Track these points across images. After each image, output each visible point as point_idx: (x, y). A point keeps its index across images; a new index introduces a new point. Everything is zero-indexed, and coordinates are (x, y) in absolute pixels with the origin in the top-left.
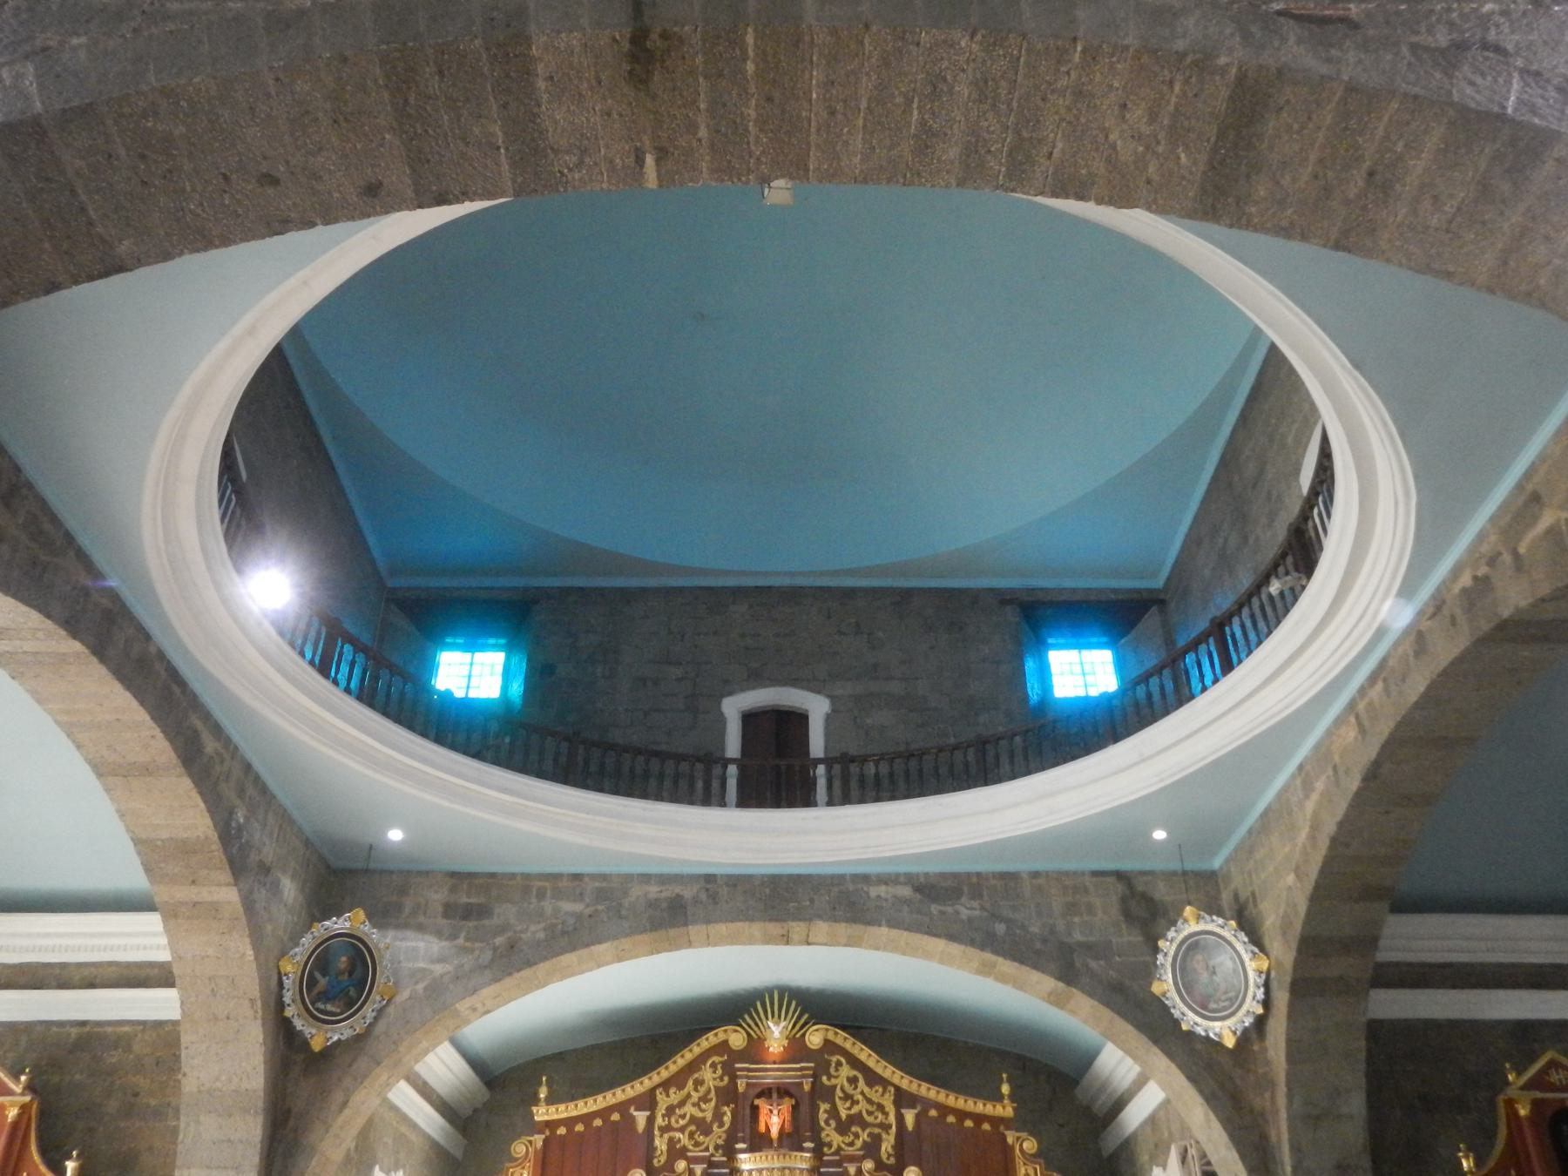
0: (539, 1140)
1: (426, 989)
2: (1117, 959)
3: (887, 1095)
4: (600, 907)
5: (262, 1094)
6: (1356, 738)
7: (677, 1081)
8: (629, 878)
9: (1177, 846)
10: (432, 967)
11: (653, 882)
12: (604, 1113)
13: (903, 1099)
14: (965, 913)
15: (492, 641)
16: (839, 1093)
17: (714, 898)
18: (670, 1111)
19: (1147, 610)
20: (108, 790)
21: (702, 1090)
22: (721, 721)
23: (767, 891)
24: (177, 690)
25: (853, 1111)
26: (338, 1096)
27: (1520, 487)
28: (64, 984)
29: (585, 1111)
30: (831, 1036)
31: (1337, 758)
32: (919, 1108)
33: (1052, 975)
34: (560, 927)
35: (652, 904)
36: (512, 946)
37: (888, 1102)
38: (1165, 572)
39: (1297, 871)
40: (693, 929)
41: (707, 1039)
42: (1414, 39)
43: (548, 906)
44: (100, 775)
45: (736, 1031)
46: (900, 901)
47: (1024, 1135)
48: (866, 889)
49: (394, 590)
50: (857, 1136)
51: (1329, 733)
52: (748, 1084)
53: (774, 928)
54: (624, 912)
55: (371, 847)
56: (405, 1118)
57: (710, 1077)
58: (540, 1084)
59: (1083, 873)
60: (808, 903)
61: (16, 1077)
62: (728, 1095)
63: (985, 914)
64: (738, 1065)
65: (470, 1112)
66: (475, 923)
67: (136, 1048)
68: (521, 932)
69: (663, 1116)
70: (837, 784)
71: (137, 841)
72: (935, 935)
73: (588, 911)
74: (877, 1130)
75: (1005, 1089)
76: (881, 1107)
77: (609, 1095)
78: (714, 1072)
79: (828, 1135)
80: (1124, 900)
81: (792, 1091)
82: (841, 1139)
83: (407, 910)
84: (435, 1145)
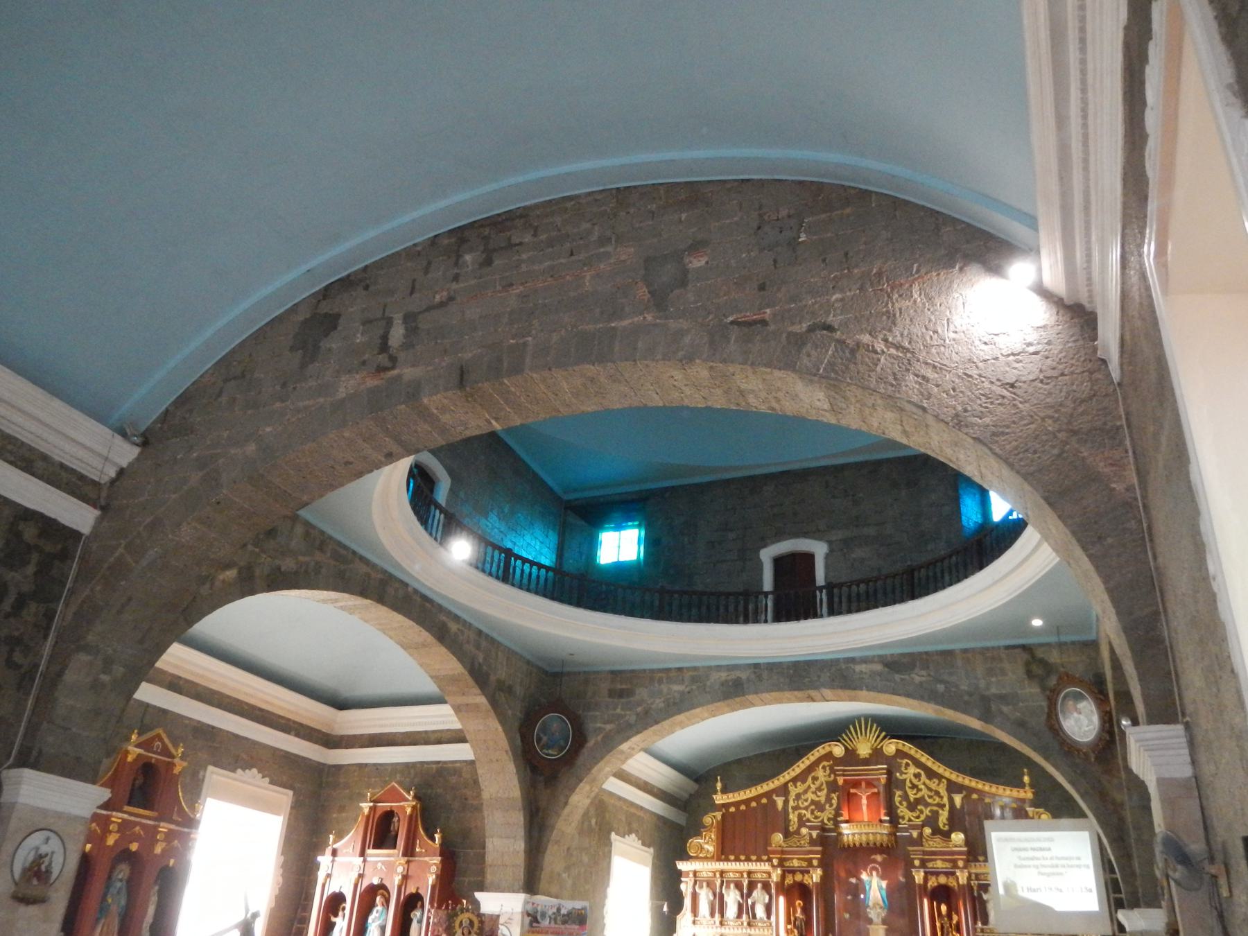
0: (719, 815)
2: (1021, 704)
3: (941, 785)
4: (694, 687)
7: (801, 778)
8: (710, 668)
9: (1054, 627)
10: (602, 726)
12: (757, 798)
13: (953, 787)
14: (917, 679)
15: (630, 524)
16: (908, 784)
17: (759, 677)
18: (798, 797)
21: (818, 783)
22: (759, 566)
23: (791, 671)
24: (428, 605)
26: (562, 799)
28: (427, 743)
29: (745, 797)
30: (900, 747)
32: (964, 793)
35: (722, 684)
36: (647, 712)
37: (942, 790)
41: (818, 751)
42: (790, 329)
44: (405, 649)
45: (836, 745)
46: (873, 674)
47: (1041, 810)
49: (569, 501)
50: (921, 812)
52: (845, 780)
54: (708, 690)
55: (563, 661)
56: (632, 804)
57: (821, 774)
58: (717, 781)
59: (999, 648)
62: (833, 787)
63: (931, 679)
64: (836, 768)
65: (686, 796)
67: (463, 774)
68: (652, 704)
69: (794, 800)
71: (432, 677)
73: (687, 689)
74: (935, 808)
75: (1026, 779)
76: (937, 793)
77: (759, 788)
80: (1027, 664)
81: (875, 783)
82: (910, 814)
84: (660, 818)
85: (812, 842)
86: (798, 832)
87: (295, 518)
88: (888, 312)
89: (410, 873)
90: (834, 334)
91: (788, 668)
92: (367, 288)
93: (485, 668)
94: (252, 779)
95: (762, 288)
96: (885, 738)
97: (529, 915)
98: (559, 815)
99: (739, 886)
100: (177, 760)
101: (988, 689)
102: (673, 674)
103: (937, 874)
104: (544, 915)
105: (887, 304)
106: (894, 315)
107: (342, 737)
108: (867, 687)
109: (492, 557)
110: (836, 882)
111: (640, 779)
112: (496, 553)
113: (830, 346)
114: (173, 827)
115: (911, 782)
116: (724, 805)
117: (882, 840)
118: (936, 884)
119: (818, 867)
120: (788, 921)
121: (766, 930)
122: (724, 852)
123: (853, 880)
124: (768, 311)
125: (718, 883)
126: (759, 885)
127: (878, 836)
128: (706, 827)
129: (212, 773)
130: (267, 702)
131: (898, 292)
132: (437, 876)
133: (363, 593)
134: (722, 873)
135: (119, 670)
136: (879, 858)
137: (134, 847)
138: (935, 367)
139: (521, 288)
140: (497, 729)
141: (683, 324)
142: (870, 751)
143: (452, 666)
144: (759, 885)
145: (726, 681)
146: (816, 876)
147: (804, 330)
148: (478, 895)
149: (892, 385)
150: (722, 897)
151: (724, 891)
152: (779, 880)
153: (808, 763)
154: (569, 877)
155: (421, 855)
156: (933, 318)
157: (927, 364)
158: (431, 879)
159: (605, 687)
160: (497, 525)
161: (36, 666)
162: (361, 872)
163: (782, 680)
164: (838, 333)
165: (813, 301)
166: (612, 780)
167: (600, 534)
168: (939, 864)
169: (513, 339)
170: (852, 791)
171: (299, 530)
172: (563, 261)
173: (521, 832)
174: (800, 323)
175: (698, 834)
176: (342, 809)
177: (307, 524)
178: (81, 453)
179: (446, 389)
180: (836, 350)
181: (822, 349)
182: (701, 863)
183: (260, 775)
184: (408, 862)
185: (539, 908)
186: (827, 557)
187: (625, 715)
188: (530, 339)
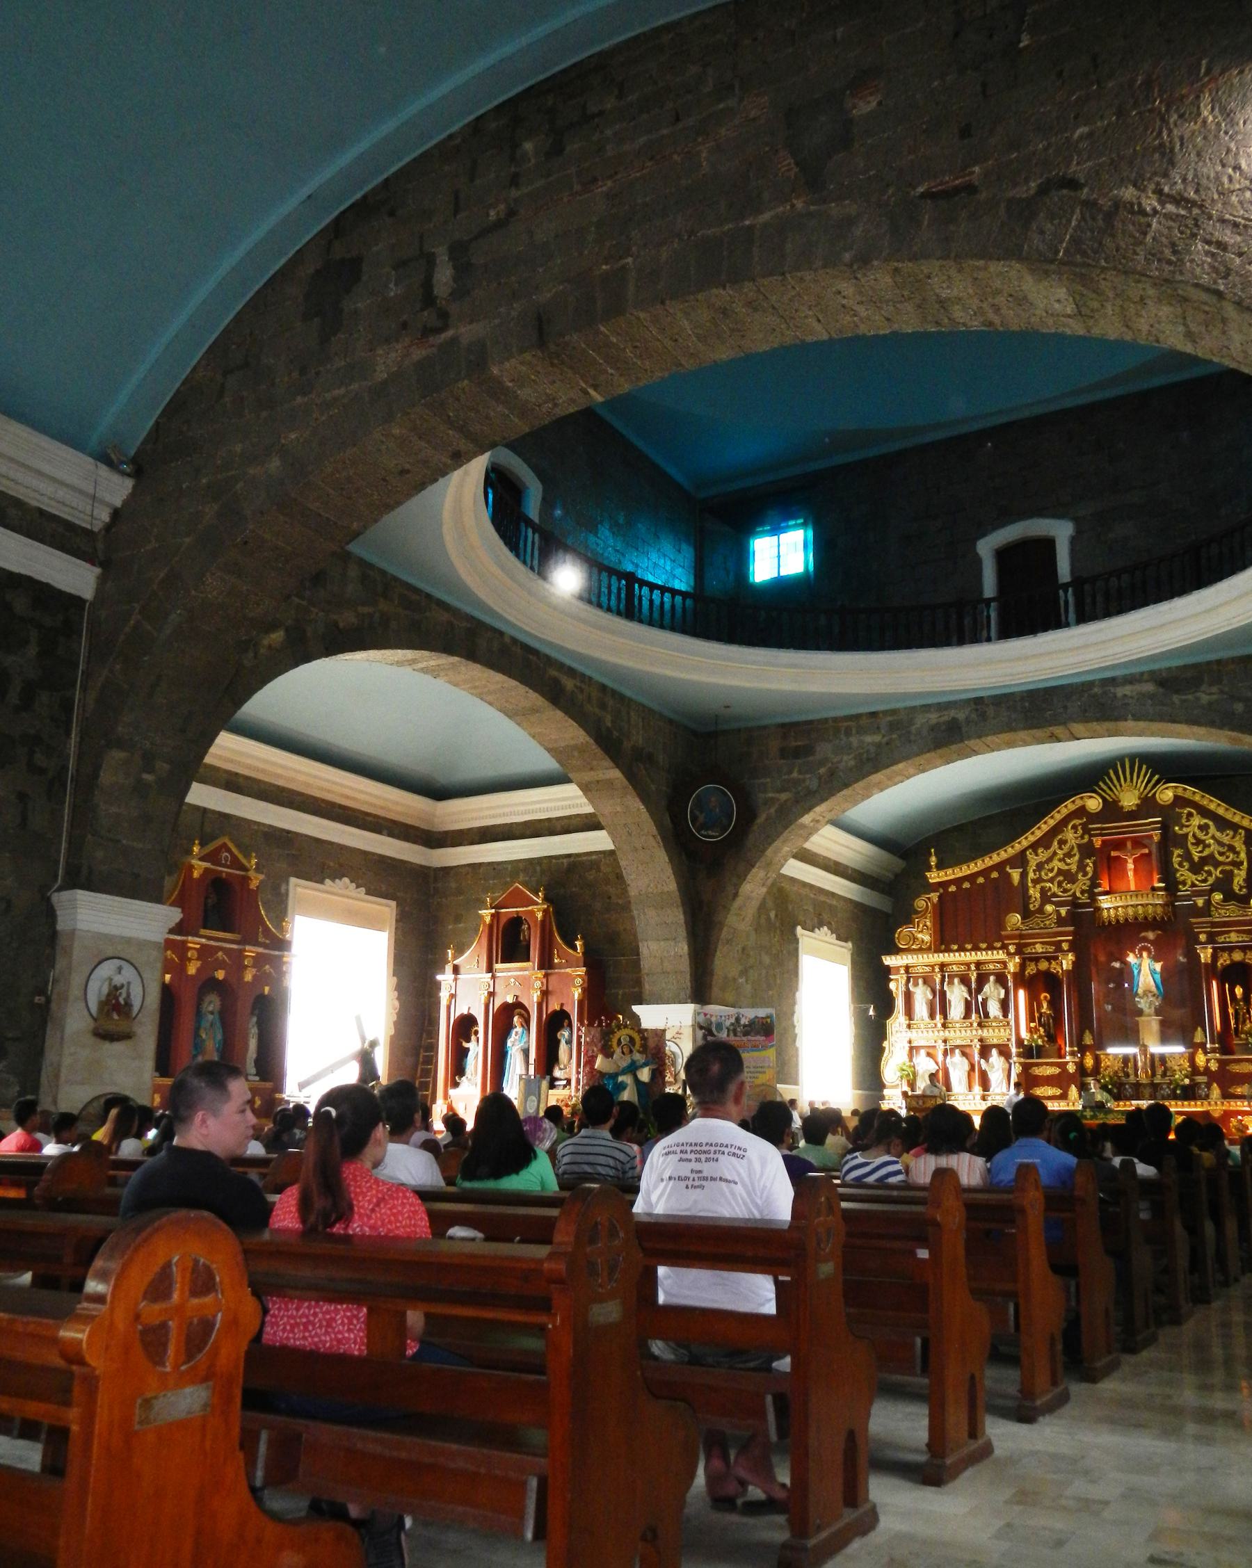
0: (935, 896)
1: (776, 811)
3: (1238, 838)
4: (894, 736)
5: (677, 893)
7: (1044, 842)
8: (914, 708)
12: (985, 872)
14: (1205, 699)
15: (792, 523)
16: (1191, 839)
17: (983, 716)
18: (1040, 867)
20: (519, 724)
21: (1066, 848)
23: (1027, 704)
25: (1206, 853)
29: (969, 872)
30: (1180, 792)
34: (865, 755)
35: (933, 729)
36: (832, 773)
41: (1066, 806)
42: (1010, 194)
44: (510, 717)
45: (1091, 797)
46: (1142, 696)
48: (1112, 690)
50: (1210, 873)
52: (1103, 841)
53: (1038, 733)
54: (913, 738)
58: (930, 854)
60: (1061, 710)
61: (537, 896)
62: (1086, 850)
65: (892, 876)
67: (602, 868)
69: (1034, 871)
71: (549, 750)
73: (885, 739)
76: (1232, 848)
77: (987, 859)
78: (1076, 833)
79: (1182, 875)
81: (1146, 841)
82: (1194, 877)
85: (1061, 921)
86: (1041, 910)
87: (346, 557)
88: (1162, 145)
89: (550, 988)
90: (1079, 192)
91: (1022, 699)
92: (392, 214)
93: (616, 734)
94: (343, 891)
95: (965, 132)
96: (1158, 782)
97: (701, 1028)
98: (727, 909)
99: (965, 981)
100: (252, 874)
102: (863, 722)
103: (1231, 950)
104: (719, 1026)
105: (1160, 133)
106: (1172, 150)
107: (446, 833)
108: (1133, 715)
109: (609, 587)
110: (1094, 970)
111: (829, 859)
112: (614, 579)
113: (1073, 213)
114: (260, 950)
115: (1194, 836)
116: (940, 884)
117: (1155, 912)
118: (1228, 962)
119: (1069, 951)
120: (1031, 1018)
121: (1002, 1030)
122: (942, 942)
123: (1117, 965)
124: (977, 169)
125: (938, 979)
126: (992, 978)
127: (1150, 909)
128: (918, 912)
129: (296, 885)
130: (348, 797)
131: (1177, 110)
132: (584, 990)
133: (448, 649)
134: (943, 966)
135: (163, 767)
136: (1151, 935)
137: (220, 975)
138: (1236, 225)
139: (609, 183)
140: (638, 810)
141: (851, 208)
142: (1137, 802)
143: (573, 734)
144: (992, 978)
146: (1067, 962)
147: (1032, 192)
148: (636, 1009)
149: (1169, 262)
150: (943, 994)
151: (946, 988)
152: (1017, 970)
153: (1052, 823)
154: (747, 981)
155: (560, 966)
156: (1233, 146)
157: (1223, 221)
158: (577, 993)
159: (774, 745)
160: (611, 542)
161: (65, 768)
162: (491, 990)
163: (1013, 716)
164: (1086, 190)
165: (1045, 143)
166: (792, 862)
167: (751, 542)
168: (1233, 937)
169: (606, 264)
170: (1113, 854)
171: (353, 572)
172: (665, 132)
173: (682, 933)
174: (1027, 180)
175: (908, 921)
176: (458, 919)
177: (362, 563)
178: (61, 493)
179: (522, 351)
180: (1083, 218)
181: (1060, 219)
182: (915, 956)
183: (354, 885)
184: (546, 976)
185: (713, 1019)
187: (804, 781)
188: (630, 260)
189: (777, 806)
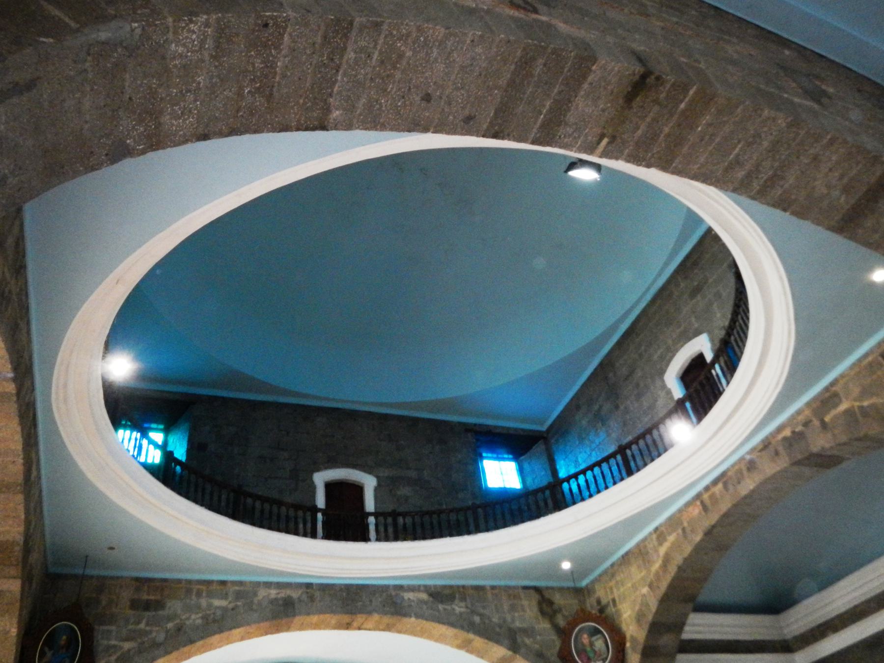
2: (538, 637)
4: (239, 603)
6: (700, 513)
8: (258, 584)
11: (273, 587)
14: (458, 610)
17: (312, 598)
19: (536, 443)
22: (313, 488)
27: (827, 389)
31: (685, 524)
33: (505, 647)
34: (212, 616)
35: (273, 602)
36: (179, 629)
38: (549, 422)
39: (651, 586)
40: (298, 620)
43: (203, 602)
46: (421, 602)
51: (680, 511)
53: (346, 618)
54: (254, 607)
63: (469, 610)
66: (154, 613)
70: (382, 529)
72: (444, 623)
73: (231, 606)
80: (540, 604)
83: (104, 603)
91: (341, 590)
101: (513, 621)
102: (214, 587)
145: (276, 599)
159: (126, 595)
163: (335, 602)
186: (376, 490)
187: (151, 632)
189: (119, 654)
